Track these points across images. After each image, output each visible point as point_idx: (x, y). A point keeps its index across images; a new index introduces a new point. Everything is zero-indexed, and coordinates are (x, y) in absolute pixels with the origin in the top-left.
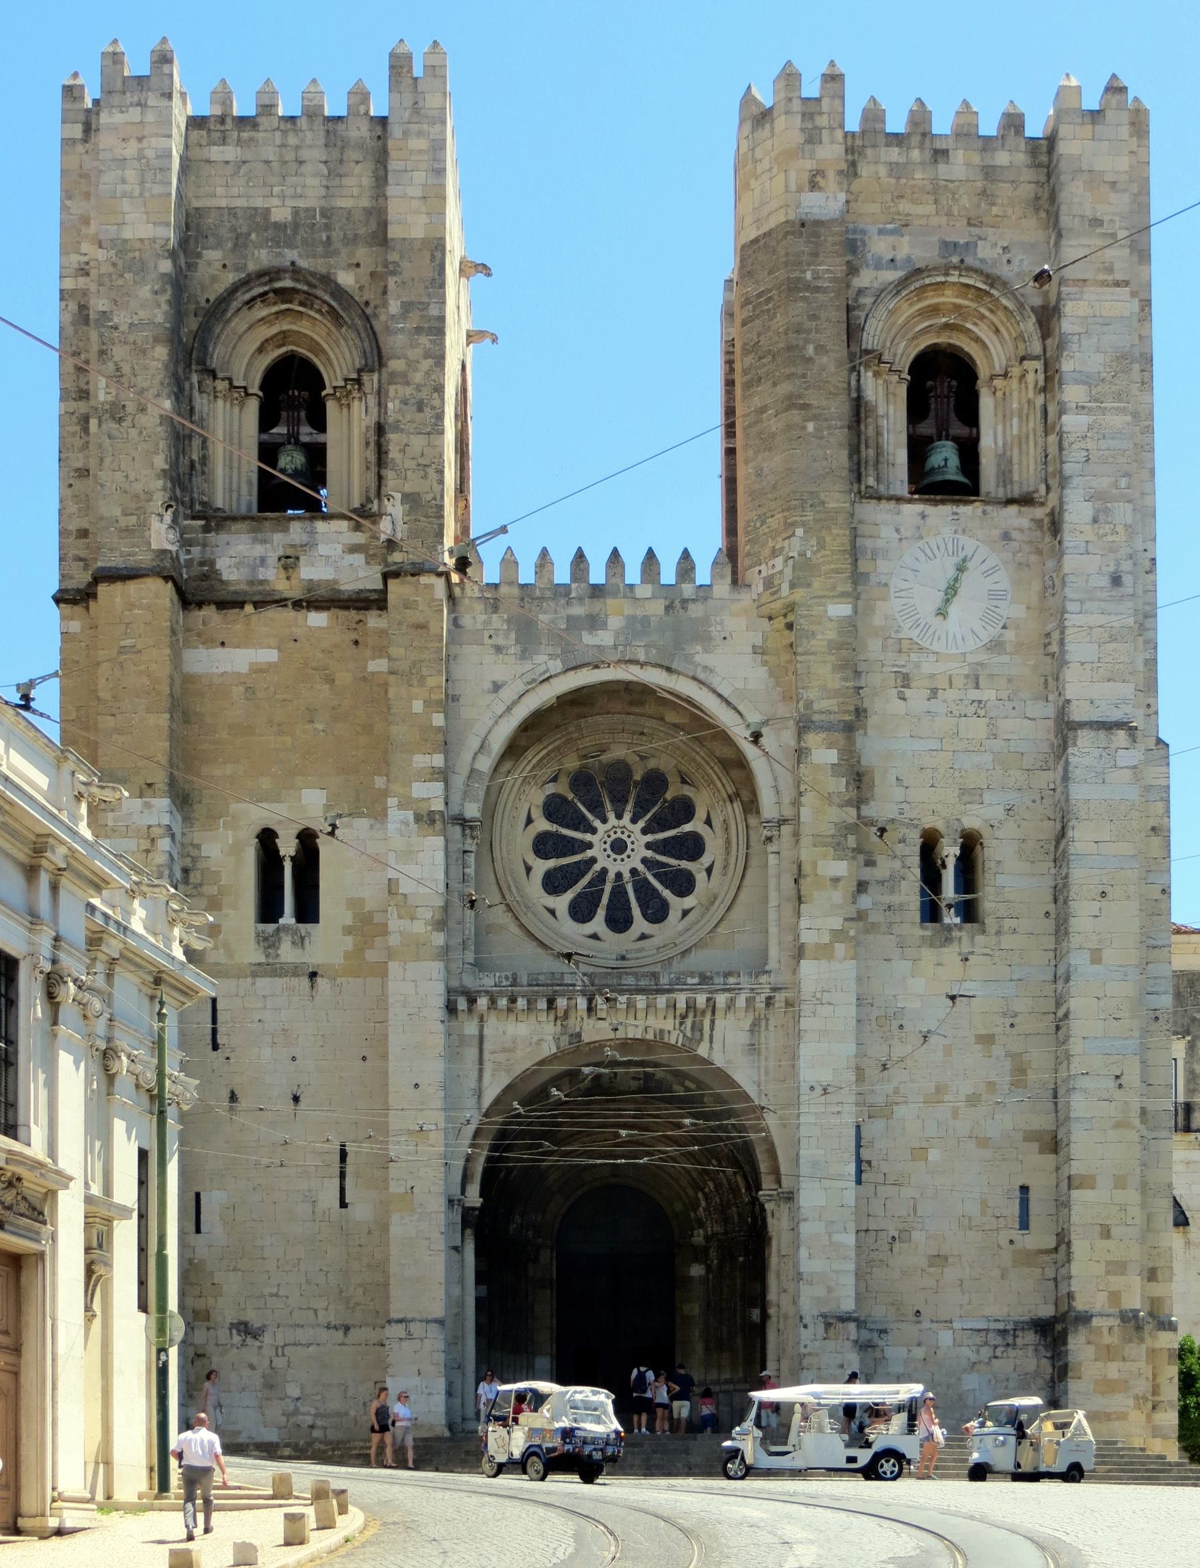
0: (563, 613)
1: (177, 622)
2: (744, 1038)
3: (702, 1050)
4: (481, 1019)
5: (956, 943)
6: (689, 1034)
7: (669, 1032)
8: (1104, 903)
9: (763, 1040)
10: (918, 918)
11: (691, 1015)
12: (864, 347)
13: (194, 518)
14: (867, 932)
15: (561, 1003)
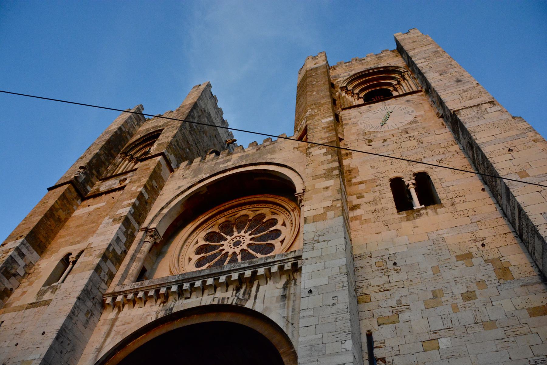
0: (214, 163)
1: (73, 200)
2: (279, 292)
3: (249, 305)
4: (120, 310)
5: (425, 215)
6: (241, 297)
7: (228, 298)
8: (513, 153)
9: (292, 291)
10: (395, 210)
11: (244, 287)
12: (340, 87)
13: (100, 180)
14: (361, 224)
15: (163, 290)
